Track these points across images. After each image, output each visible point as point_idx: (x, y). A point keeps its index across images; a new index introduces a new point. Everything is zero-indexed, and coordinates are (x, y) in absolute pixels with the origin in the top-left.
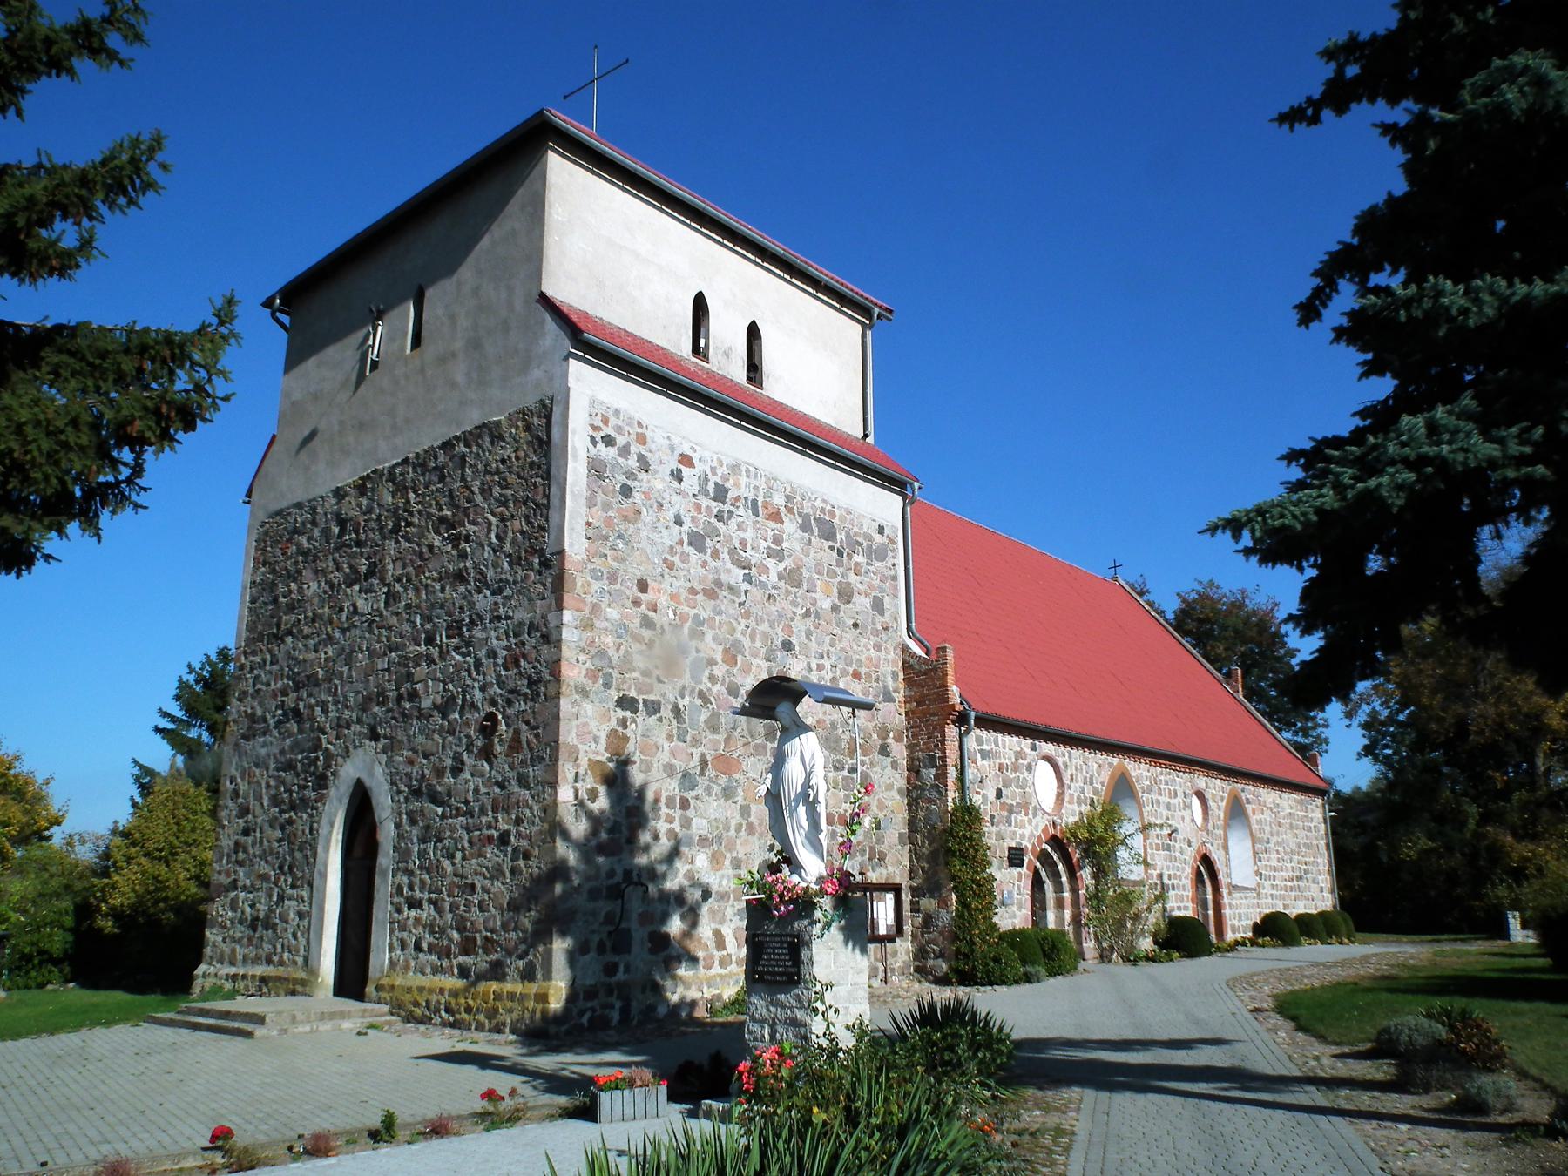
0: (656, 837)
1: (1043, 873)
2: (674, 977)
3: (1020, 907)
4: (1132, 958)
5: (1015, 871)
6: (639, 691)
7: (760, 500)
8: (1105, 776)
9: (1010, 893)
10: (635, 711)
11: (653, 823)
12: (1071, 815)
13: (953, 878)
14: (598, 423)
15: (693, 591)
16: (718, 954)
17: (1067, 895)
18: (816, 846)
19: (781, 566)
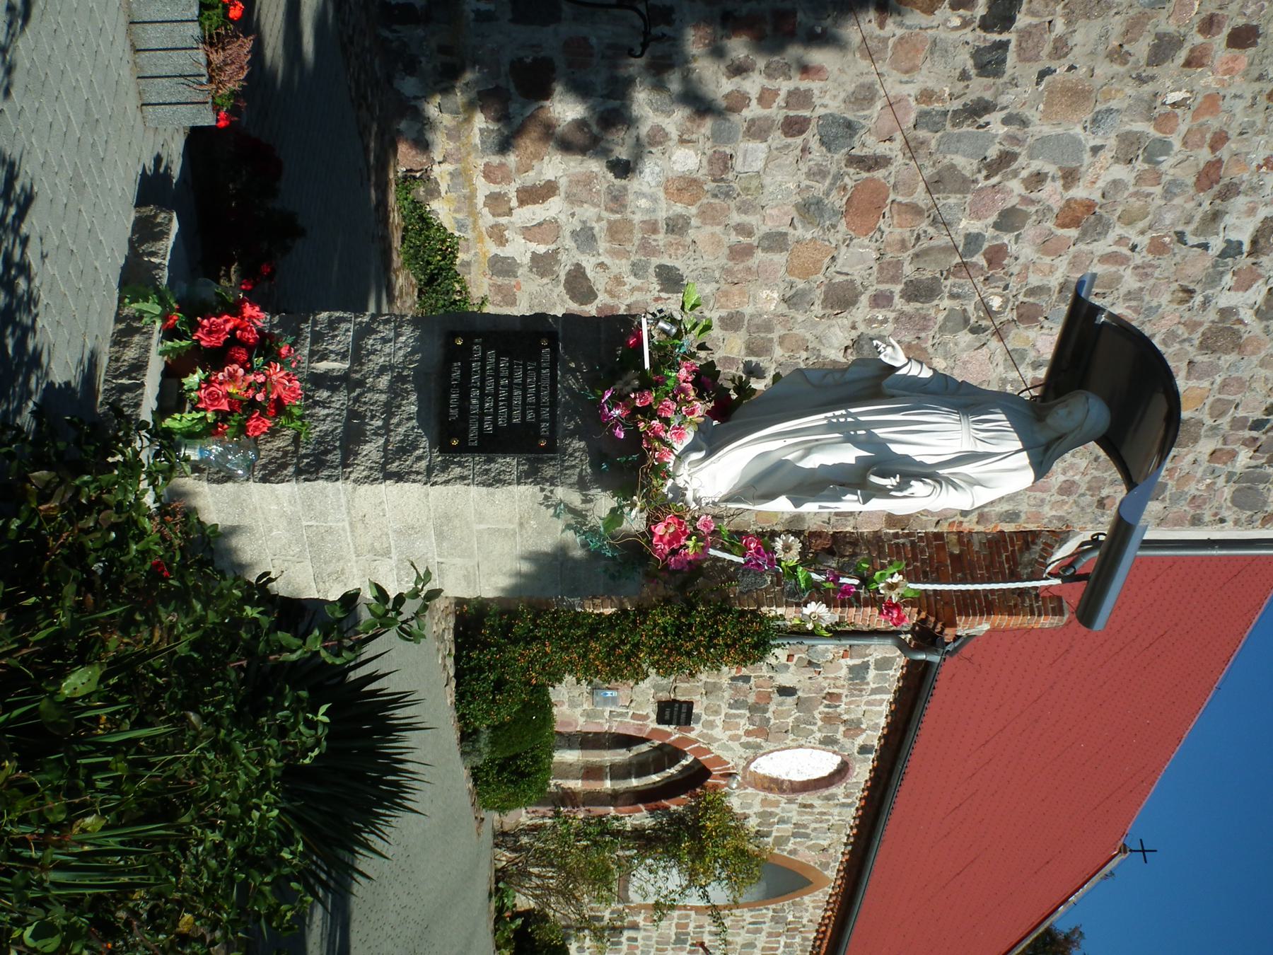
0: (738, 70)
1: (645, 748)
2: (470, 107)
3: (588, 715)
4: (503, 879)
5: (651, 711)
6: (1026, 34)
8: (806, 856)
9: (614, 701)
10: (986, 25)
11: (761, 63)
12: (742, 801)
13: (642, 611)
15: (1219, 139)
16: (511, 190)
17: (608, 784)
18: (761, 485)
19: (1247, 315)
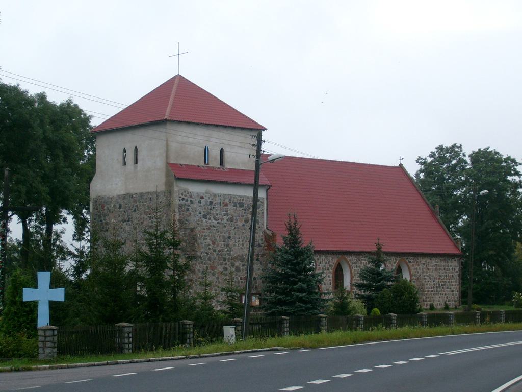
7: (222, 202)
14: (180, 196)
